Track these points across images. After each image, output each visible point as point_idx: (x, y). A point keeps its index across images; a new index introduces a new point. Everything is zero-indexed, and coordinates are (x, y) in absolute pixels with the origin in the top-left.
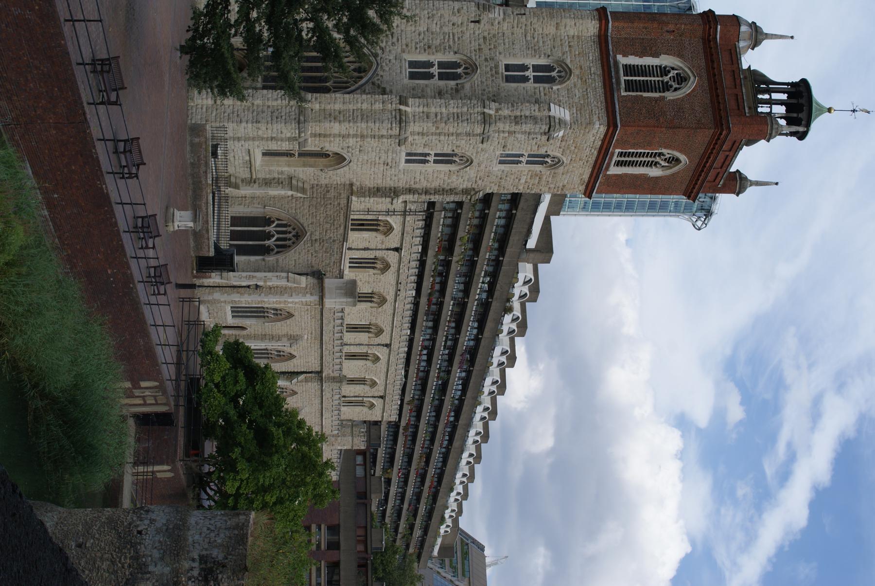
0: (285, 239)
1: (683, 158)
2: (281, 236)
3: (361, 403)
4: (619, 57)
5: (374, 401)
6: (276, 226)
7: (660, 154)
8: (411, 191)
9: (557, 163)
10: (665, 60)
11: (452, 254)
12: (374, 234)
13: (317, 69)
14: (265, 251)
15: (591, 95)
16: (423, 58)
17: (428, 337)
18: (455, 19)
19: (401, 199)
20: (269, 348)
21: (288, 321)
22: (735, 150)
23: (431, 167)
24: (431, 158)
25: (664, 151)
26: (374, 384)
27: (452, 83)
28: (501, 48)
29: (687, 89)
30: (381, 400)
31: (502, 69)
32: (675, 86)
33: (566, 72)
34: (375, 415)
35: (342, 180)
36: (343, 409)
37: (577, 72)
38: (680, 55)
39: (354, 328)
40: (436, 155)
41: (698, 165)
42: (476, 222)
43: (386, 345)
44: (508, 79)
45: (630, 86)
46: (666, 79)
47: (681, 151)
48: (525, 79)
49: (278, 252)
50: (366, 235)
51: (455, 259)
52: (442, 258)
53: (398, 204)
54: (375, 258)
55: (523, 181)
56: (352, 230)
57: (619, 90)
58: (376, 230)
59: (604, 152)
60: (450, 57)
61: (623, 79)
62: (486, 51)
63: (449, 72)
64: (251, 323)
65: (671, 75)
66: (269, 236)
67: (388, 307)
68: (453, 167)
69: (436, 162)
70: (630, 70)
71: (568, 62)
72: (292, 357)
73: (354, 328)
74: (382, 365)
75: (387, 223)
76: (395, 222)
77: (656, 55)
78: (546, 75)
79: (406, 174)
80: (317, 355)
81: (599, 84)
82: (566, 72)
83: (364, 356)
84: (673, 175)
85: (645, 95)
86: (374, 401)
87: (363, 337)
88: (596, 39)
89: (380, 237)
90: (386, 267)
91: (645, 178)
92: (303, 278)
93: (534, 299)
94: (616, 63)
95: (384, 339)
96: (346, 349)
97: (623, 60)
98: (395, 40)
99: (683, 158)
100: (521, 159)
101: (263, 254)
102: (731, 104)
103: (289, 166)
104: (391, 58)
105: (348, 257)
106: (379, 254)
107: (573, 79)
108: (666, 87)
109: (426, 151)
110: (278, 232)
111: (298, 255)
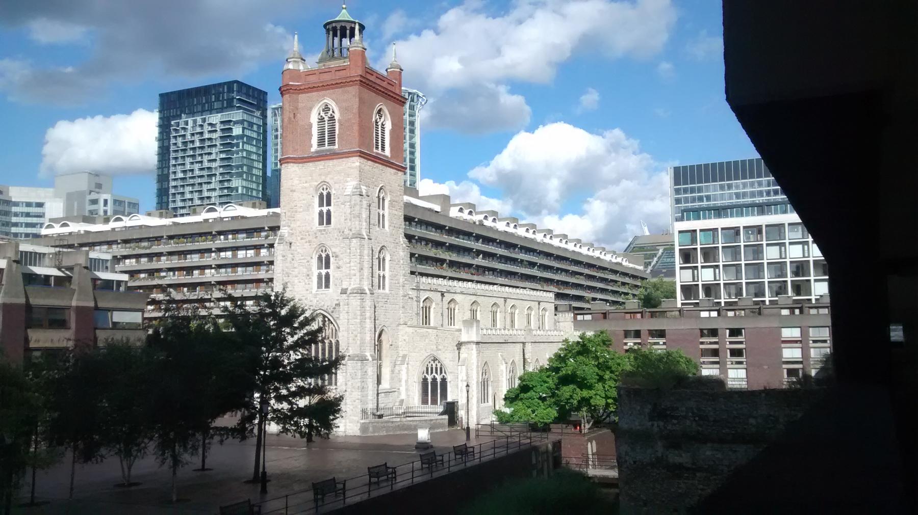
10: (314, 119)
11: (445, 260)
14: (444, 382)
15: (338, 168)
18: (289, 259)
27: (332, 260)
28: (309, 228)
29: (333, 105)
31: (322, 228)
32: (331, 112)
37: (323, 178)
38: (310, 109)
45: (332, 142)
46: (326, 119)
55: (396, 213)
59: (377, 159)
60: (315, 262)
61: (327, 147)
62: (310, 238)
63: (325, 262)
66: (434, 379)
70: (321, 142)
76: (424, 295)
77: (310, 126)
81: (330, 163)
92: (462, 356)
94: (317, 152)
97: (315, 147)
108: (332, 118)
110: (432, 373)
111: (447, 358)
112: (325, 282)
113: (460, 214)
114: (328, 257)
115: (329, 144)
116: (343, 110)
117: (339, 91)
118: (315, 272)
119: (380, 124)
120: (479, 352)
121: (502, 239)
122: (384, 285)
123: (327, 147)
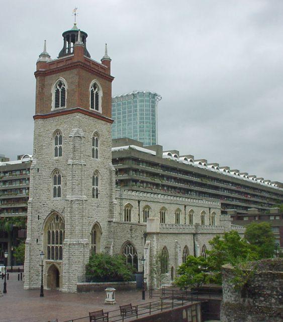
0: (131, 250)
1: (93, 82)
2: (130, 251)
3: (213, 218)
4: (52, 110)
5: (211, 213)
6: (131, 253)
7: (92, 91)
8: (111, 196)
9: (96, 134)
12: (132, 212)
13: (57, 236)
16: (52, 191)
17: (195, 193)
19: (114, 200)
20: (181, 256)
21: (168, 248)
22: (90, 61)
23: (99, 187)
24: (95, 187)
25: (90, 89)
26: (204, 212)
28: (49, 159)
30: (211, 209)
32: (62, 86)
33: (58, 131)
34: (218, 212)
35: (106, 225)
36: (216, 225)
37: (58, 127)
39: (178, 220)
40: (93, 185)
41: (96, 75)
42: (145, 175)
43: (185, 207)
44: (60, 155)
45: (63, 105)
46: (60, 90)
47: (90, 82)
48: (60, 148)
49: (137, 253)
50: (132, 215)
51: (160, 183)
52: (161, 188)
53: (115, 201)
54: (144, 211)
56: (130, 221)
57: (64, 109)
58: (130, 210)
59: (91, 114)
60: (52, 180)
63: (57, 180)
64: (171, 263)
65: (59, 88)
67: (167, 206)
68: (100, 178)
69: (97, 185)
70: (57, 105)
71: (54, 131)
72: (186, 247)
73: (178, 220)
74: (195, 209)
75: (127, 206)
76: (125, 203)
77: (51, 95)
78: (58, 139)
79: (103, 199)
80: (185, 236)
81: (62, 117)
82: (58, 131)
83: (191, 217)
84: (102, 87)
85: (66, 98)
86: (211, 213)
87: (182, 217)
88: (45, 120)
89: (133, 209)
90: (147, 206)
91: (103, 98)
93: (177, 152)
94: (54, 111)
95: (182, 208)
96: (188, 223)
97: (53, 109)
98: (45, 203)
99: (93, 82)
100: (95, 149)
101: (137, 259)
102: (69, 62)
103: (99, 248)
104: (52, 204)
105: (143, 223)
106: (141, 210)
107: (60, 128)
108: (63, 90)
109: (91, 189)
110: (128, 253)
111: (137, 243)
112: (57, 193)
113: (169, 157)
114: (60, 177)
115: (61, 106)
116: (70, 84)
117: (67, 72)
118: (52, 186)
119: (95, 92)
120: (158, 240)
121: (210, 175)
122: (97, 196)
123: (60, 108)
